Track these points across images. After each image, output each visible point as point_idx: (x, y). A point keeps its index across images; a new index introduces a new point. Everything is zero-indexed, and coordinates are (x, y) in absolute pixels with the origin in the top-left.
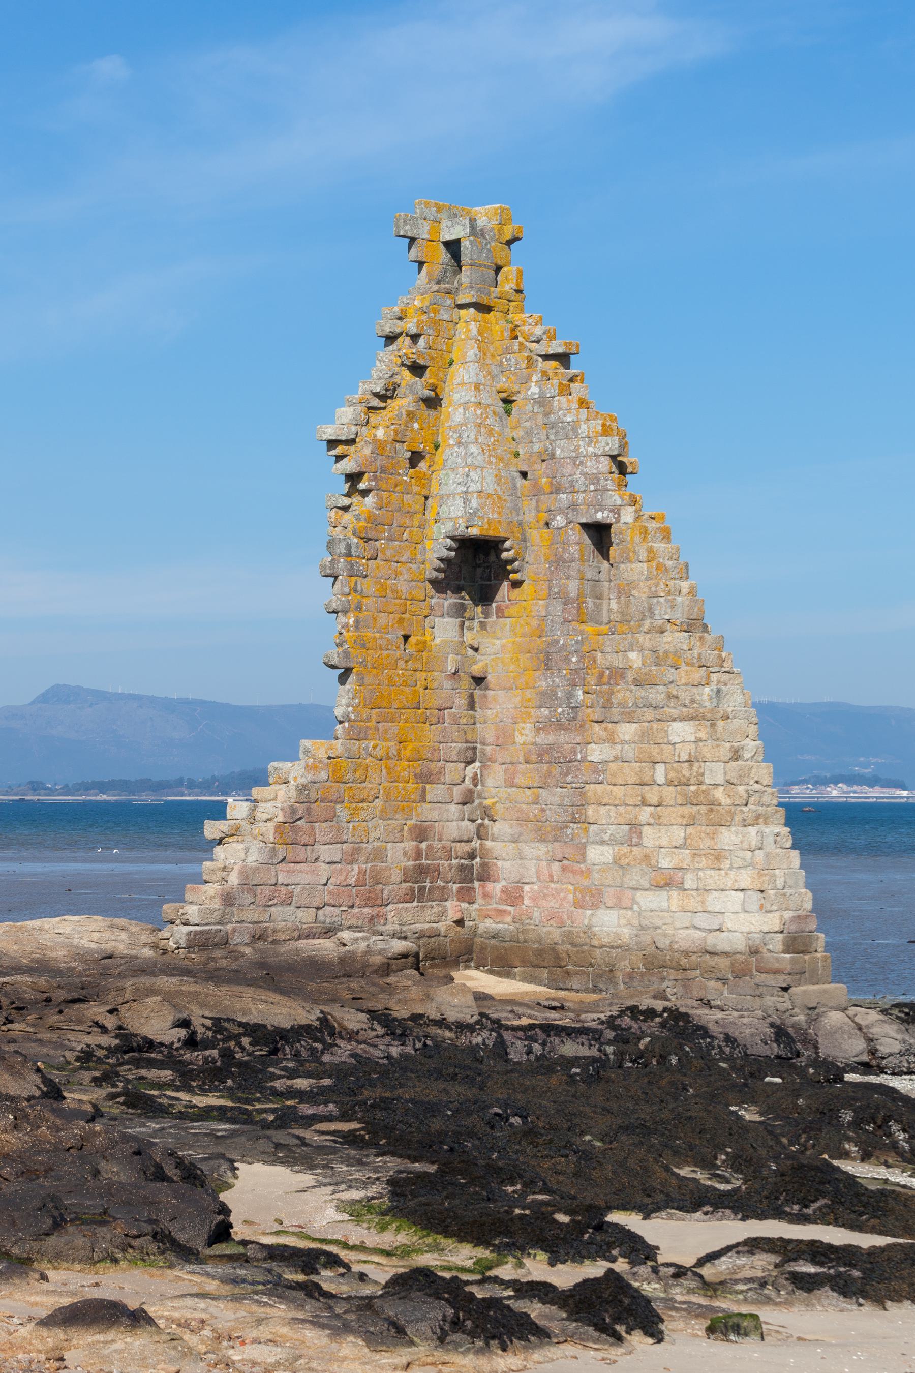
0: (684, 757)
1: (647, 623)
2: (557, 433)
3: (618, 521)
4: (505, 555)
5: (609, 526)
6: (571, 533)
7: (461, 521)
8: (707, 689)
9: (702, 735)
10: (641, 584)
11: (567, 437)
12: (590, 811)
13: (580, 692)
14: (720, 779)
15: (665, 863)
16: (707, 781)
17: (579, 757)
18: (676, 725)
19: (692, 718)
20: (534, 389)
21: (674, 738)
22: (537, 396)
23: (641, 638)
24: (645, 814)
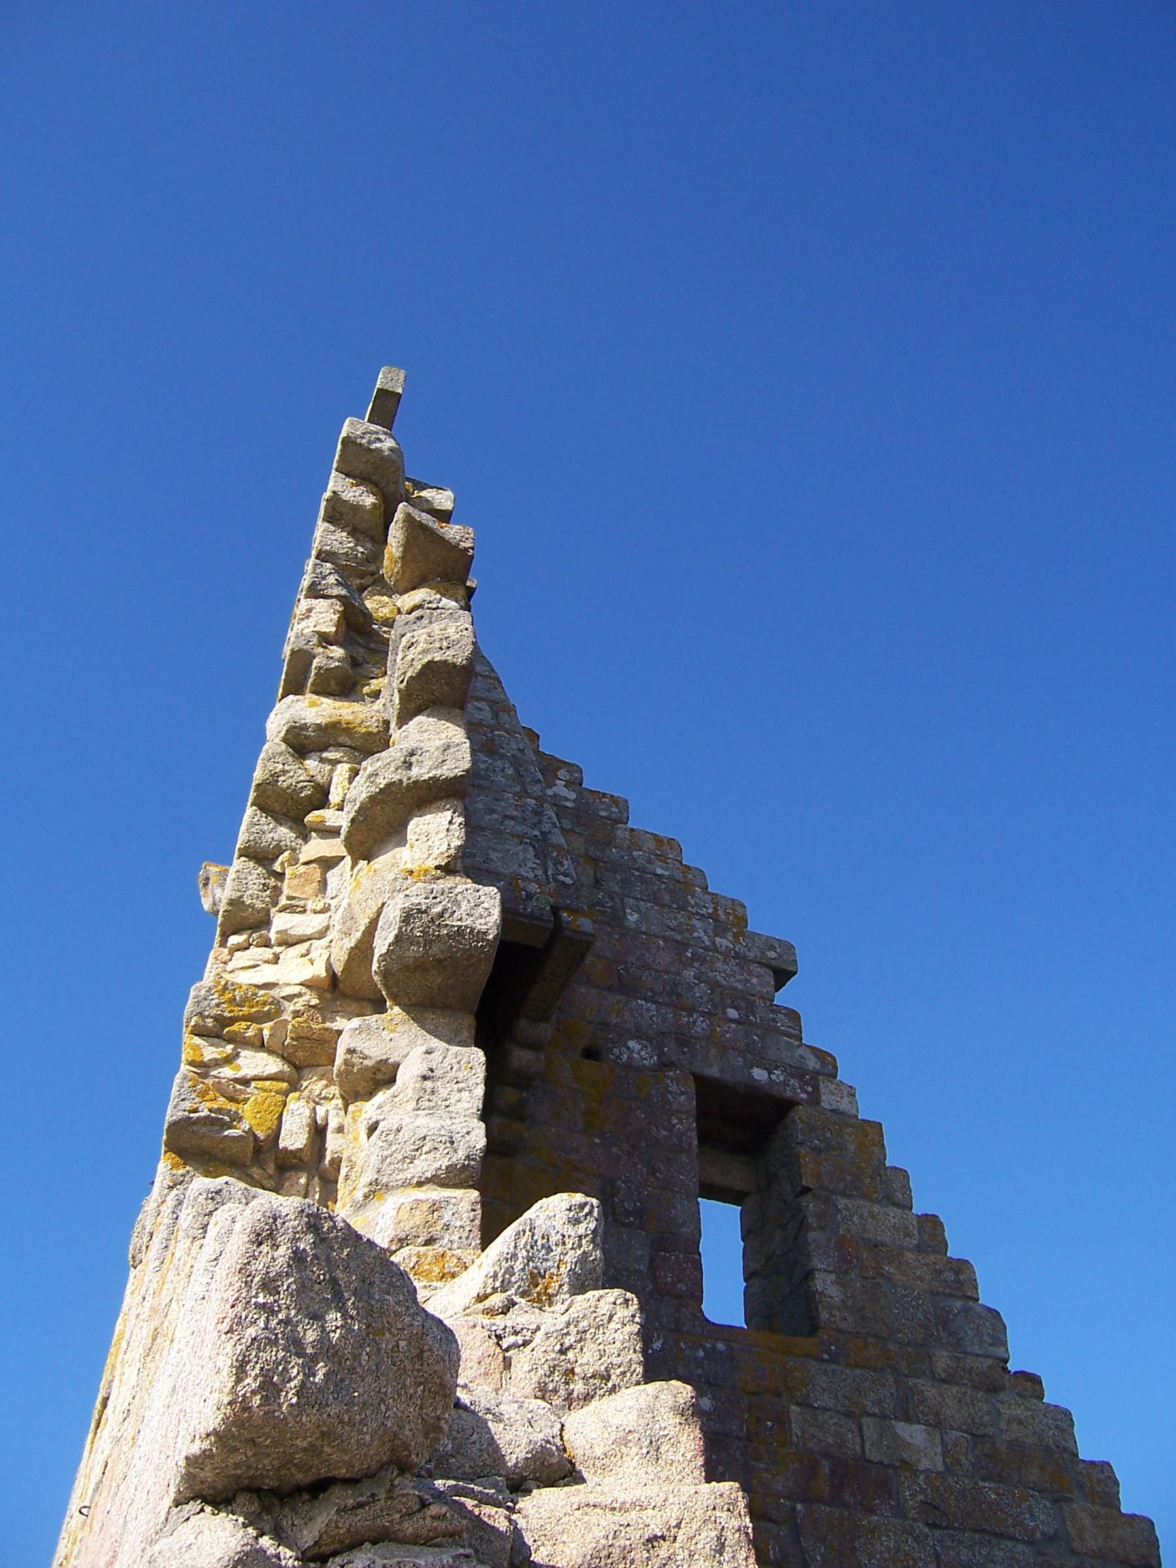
2: (625, 882)
3: (815, 1099)
5: (792, 1104)
6: (674, 1088)
7: (533, 888)
10: (909, 1256)
11: (655, 899)
22: (568, 804)
23: (931, 1391)
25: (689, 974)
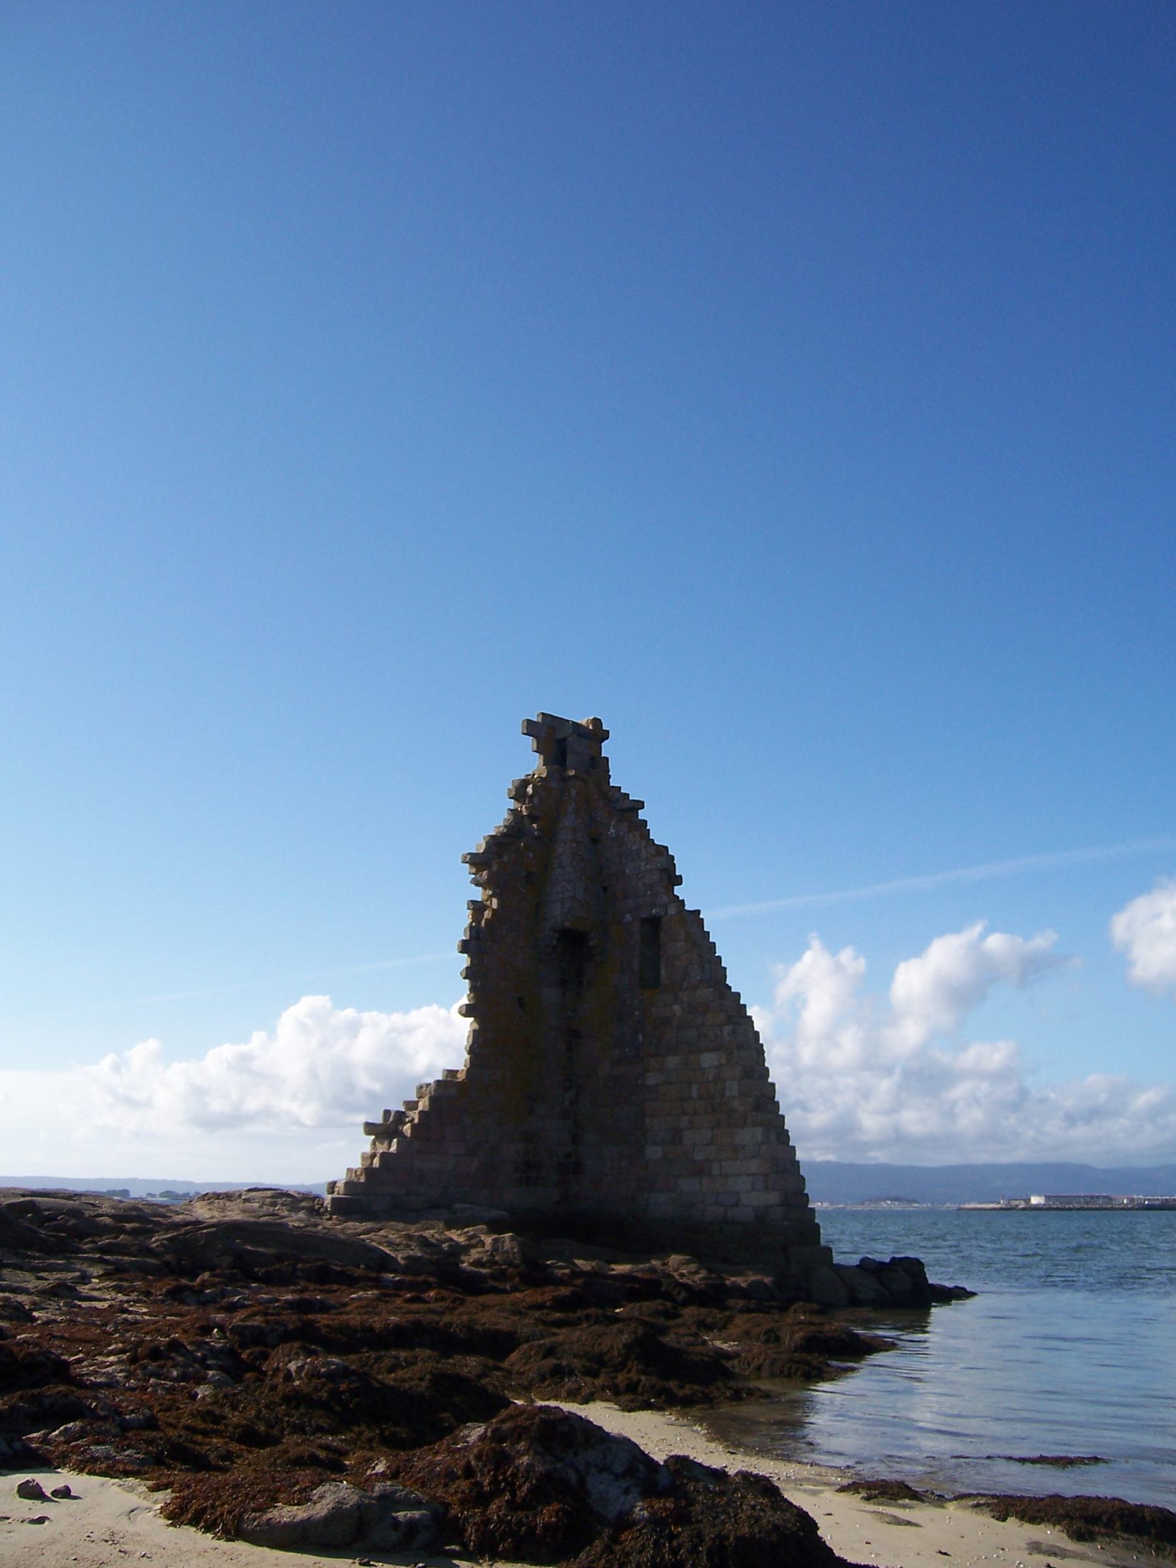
0: (711, 1078)
1: (686, 984)
3: (666, 913)
4: (591, 943)
8: (727, 1029)
12: (648, 1121)
13: (641, 1038)
14: (735, 1092)
15: (699, 1156)
16: (728, 1094)
19: (715, 1049)
20: (612, 830)
21: (705, 1065)
24: (685, 1121)
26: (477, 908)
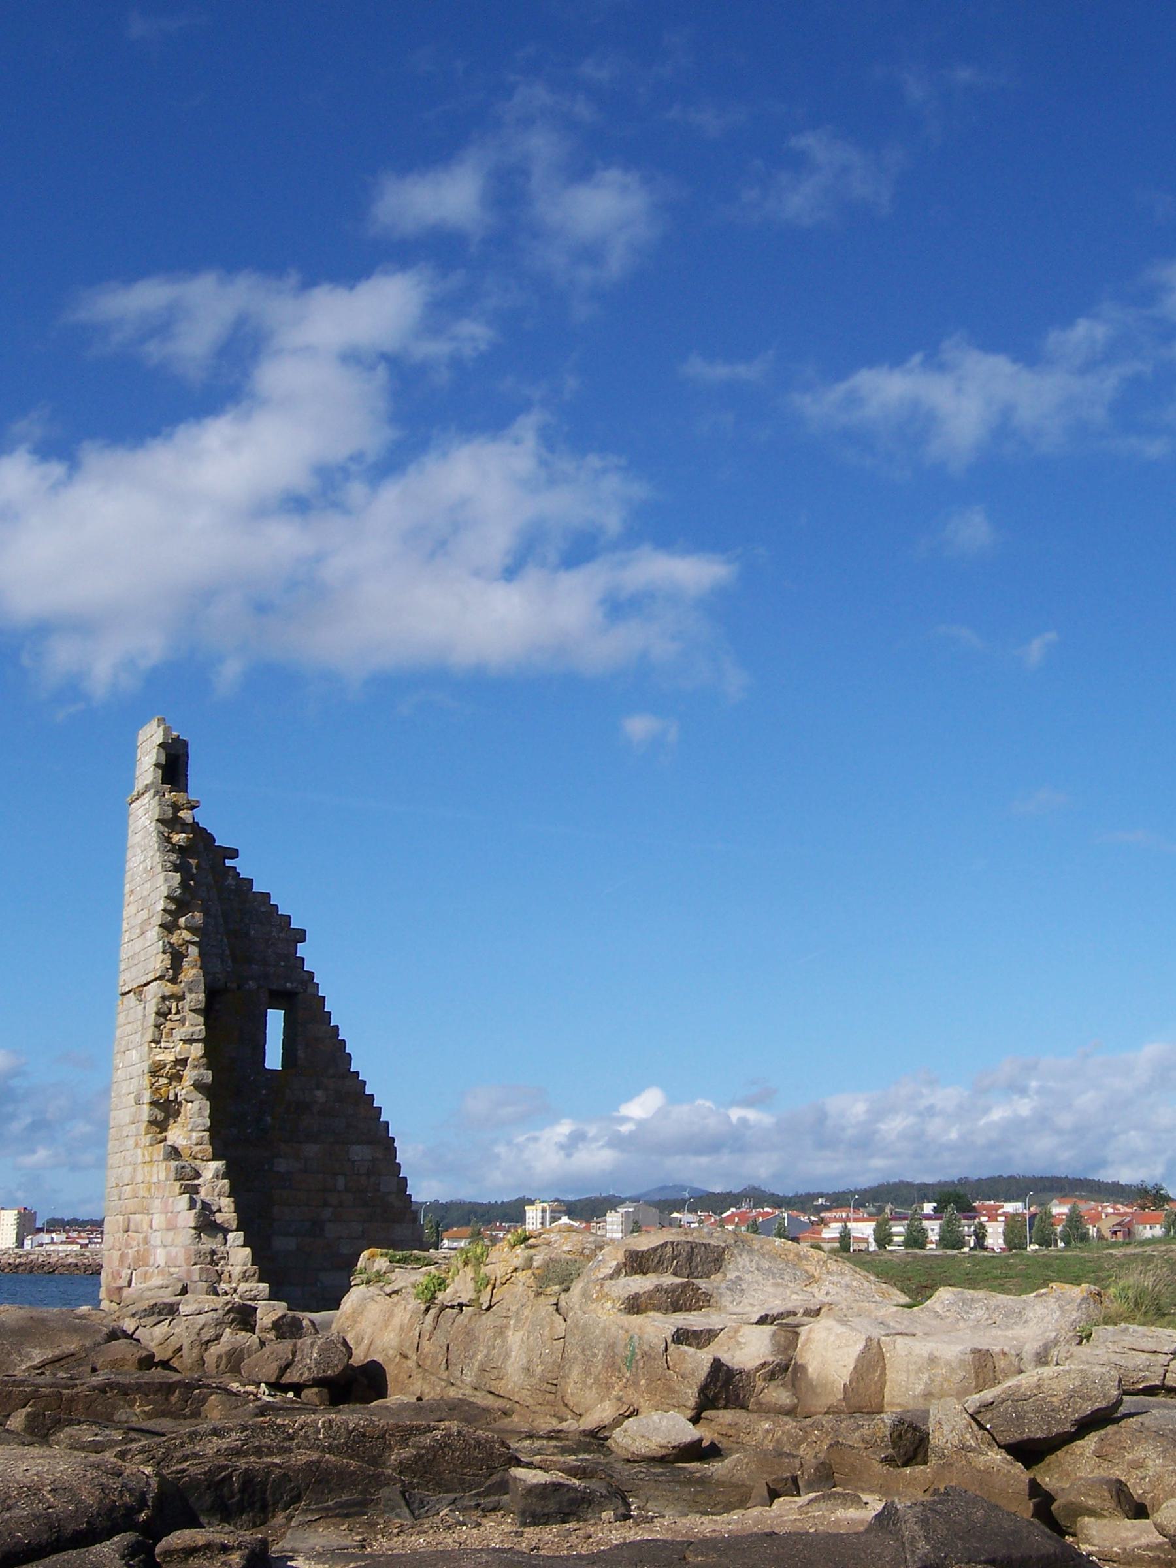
3: (305, 991)
9: (379, 1155)
13: (269, 1119)
17: (266, 1167)
18: (357, 1148)
19: (369, 1143)
24: (327, 1213)
25: (270, 951)
26: (176, 957)
